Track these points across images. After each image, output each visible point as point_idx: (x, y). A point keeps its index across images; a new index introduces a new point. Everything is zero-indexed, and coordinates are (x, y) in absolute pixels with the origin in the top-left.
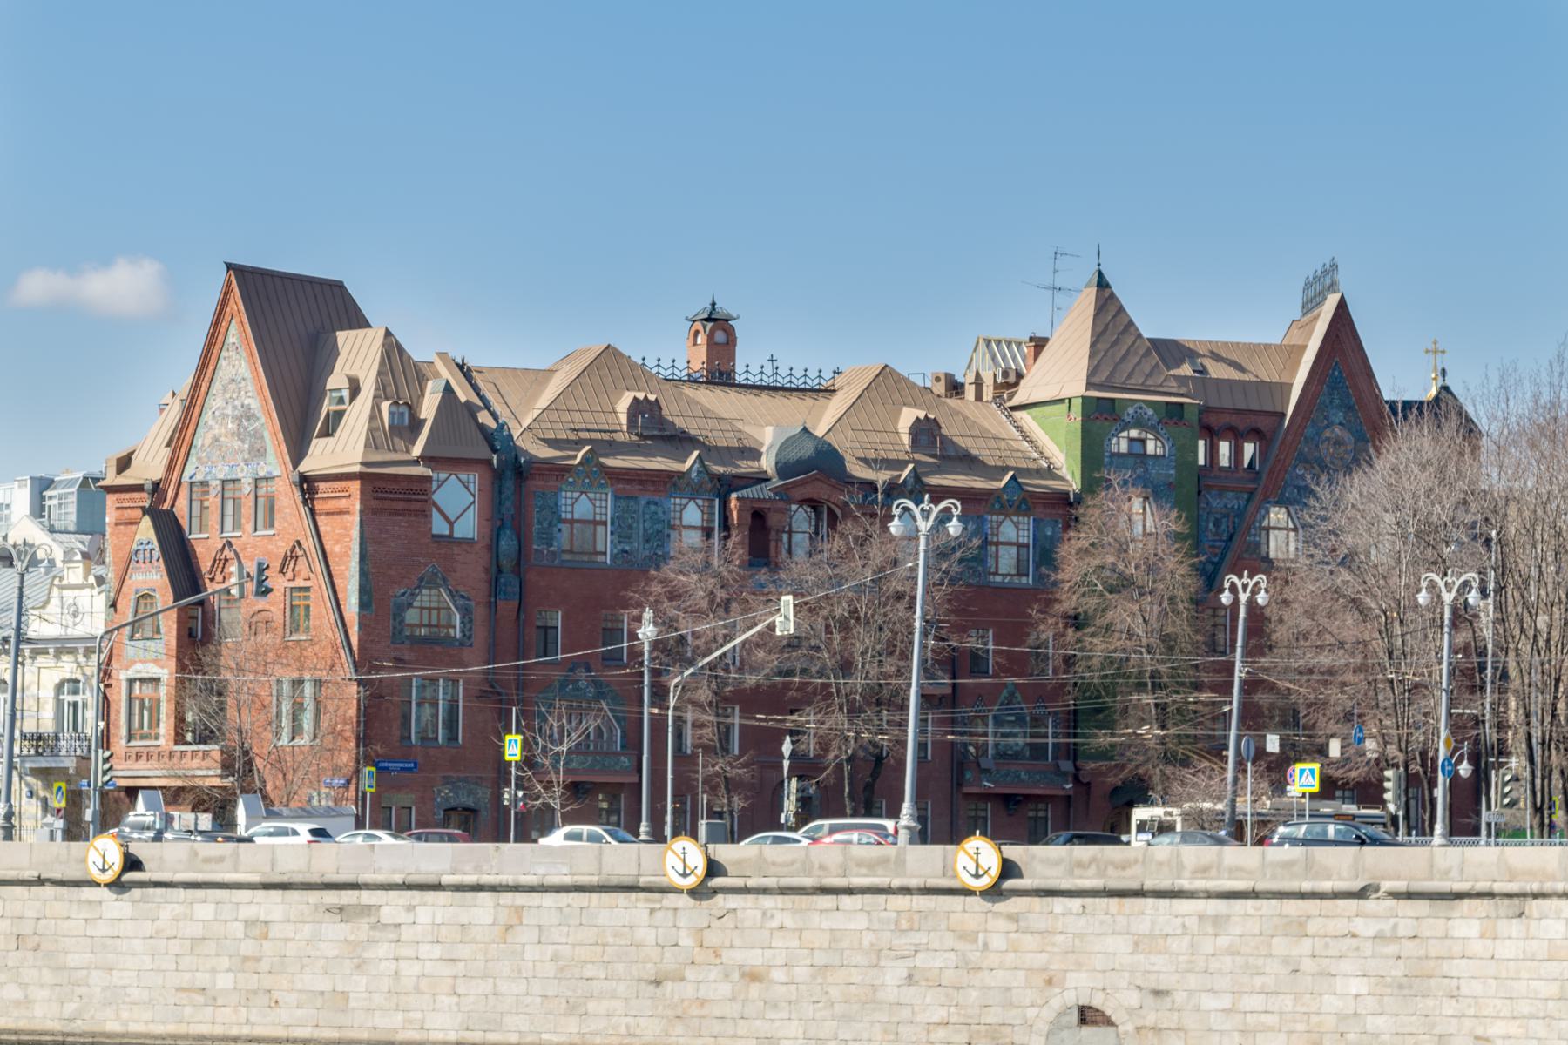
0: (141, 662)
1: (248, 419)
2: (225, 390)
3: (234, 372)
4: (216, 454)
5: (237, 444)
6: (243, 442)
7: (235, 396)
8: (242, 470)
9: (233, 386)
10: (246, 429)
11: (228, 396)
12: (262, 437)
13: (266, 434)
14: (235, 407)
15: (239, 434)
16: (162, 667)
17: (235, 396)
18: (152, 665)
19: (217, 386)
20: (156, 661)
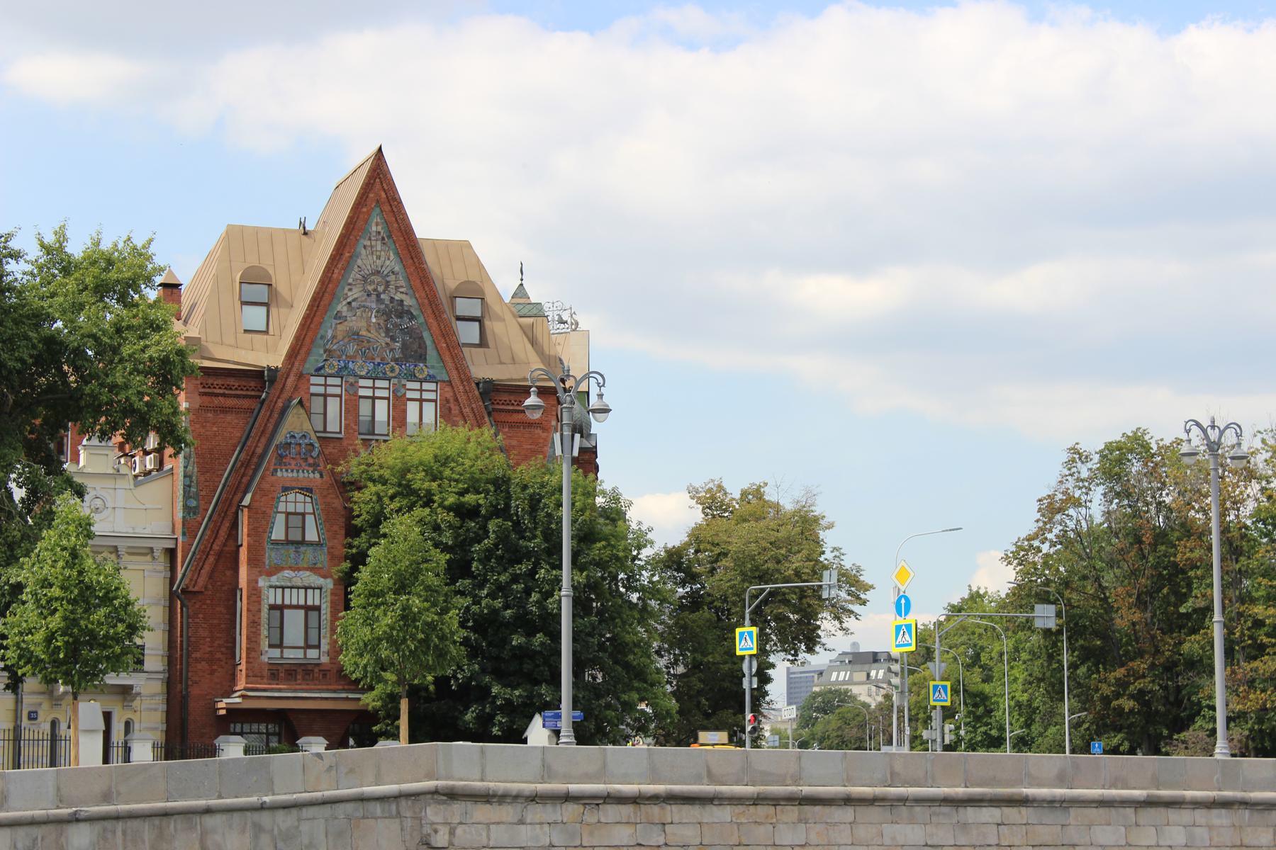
0: (291, 568)
1: (400, 316)
2: (365, 279)
3: (379, 262)
4: (352, 349)
5: (383, 339)
6: (393, 339)
7: (381, 289)
8: (392, 370)
9: (377, 279)
10: (396, 325)
11: (370, 288)
12: (422, 338)
13: (426, 335)
14: (379, 300)
15: (387, 331)
16: (325, 577)
17: (381, 289)
18: (308, 573)
19: (354, 275)
20: (313, 569)
